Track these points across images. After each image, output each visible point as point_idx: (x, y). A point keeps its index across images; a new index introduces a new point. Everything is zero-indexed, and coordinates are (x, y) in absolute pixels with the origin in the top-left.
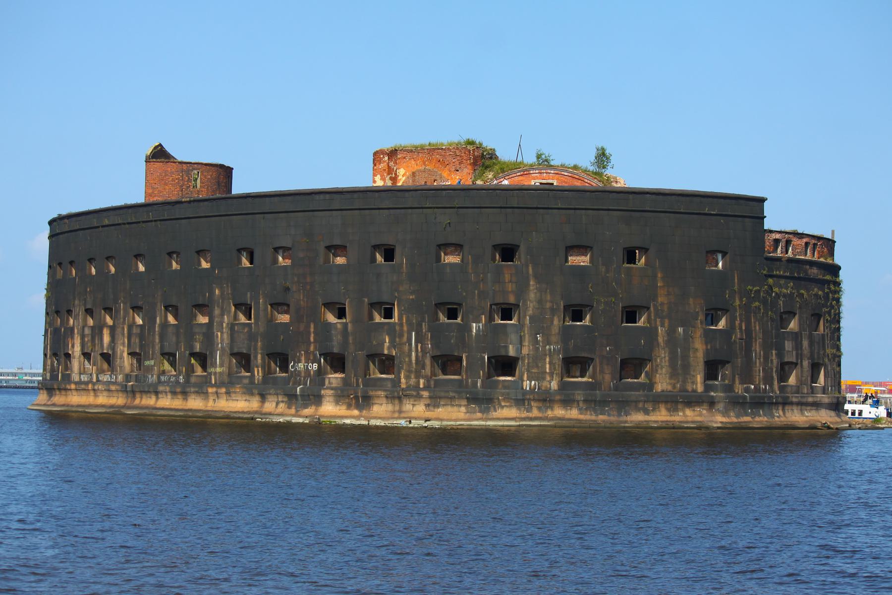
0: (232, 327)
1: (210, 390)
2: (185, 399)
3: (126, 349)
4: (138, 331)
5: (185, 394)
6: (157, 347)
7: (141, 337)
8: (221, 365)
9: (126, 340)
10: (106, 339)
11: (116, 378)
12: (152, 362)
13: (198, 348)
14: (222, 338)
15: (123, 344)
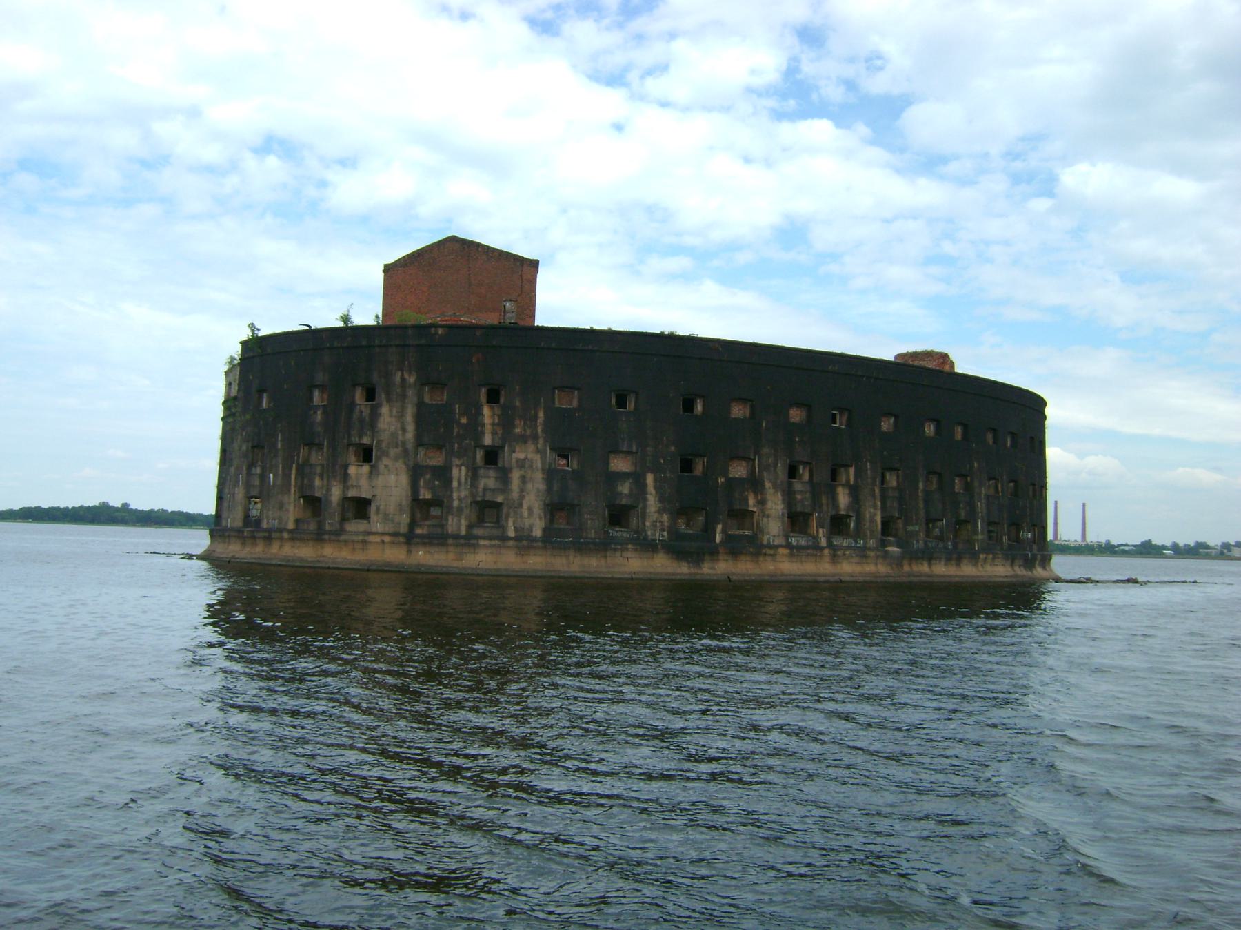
0: (988, 497)
1: (982, 556)
2: (958, 565)
3: (879, 513)
4: (897, 494)
5: (959, 561)
6: (922, 513)
9: (879, 503)
10: (843, 498)
11: (865, 542)
12: (917, 528)
13: (963, 515)
14: (981, 506)
15: (875, 507)
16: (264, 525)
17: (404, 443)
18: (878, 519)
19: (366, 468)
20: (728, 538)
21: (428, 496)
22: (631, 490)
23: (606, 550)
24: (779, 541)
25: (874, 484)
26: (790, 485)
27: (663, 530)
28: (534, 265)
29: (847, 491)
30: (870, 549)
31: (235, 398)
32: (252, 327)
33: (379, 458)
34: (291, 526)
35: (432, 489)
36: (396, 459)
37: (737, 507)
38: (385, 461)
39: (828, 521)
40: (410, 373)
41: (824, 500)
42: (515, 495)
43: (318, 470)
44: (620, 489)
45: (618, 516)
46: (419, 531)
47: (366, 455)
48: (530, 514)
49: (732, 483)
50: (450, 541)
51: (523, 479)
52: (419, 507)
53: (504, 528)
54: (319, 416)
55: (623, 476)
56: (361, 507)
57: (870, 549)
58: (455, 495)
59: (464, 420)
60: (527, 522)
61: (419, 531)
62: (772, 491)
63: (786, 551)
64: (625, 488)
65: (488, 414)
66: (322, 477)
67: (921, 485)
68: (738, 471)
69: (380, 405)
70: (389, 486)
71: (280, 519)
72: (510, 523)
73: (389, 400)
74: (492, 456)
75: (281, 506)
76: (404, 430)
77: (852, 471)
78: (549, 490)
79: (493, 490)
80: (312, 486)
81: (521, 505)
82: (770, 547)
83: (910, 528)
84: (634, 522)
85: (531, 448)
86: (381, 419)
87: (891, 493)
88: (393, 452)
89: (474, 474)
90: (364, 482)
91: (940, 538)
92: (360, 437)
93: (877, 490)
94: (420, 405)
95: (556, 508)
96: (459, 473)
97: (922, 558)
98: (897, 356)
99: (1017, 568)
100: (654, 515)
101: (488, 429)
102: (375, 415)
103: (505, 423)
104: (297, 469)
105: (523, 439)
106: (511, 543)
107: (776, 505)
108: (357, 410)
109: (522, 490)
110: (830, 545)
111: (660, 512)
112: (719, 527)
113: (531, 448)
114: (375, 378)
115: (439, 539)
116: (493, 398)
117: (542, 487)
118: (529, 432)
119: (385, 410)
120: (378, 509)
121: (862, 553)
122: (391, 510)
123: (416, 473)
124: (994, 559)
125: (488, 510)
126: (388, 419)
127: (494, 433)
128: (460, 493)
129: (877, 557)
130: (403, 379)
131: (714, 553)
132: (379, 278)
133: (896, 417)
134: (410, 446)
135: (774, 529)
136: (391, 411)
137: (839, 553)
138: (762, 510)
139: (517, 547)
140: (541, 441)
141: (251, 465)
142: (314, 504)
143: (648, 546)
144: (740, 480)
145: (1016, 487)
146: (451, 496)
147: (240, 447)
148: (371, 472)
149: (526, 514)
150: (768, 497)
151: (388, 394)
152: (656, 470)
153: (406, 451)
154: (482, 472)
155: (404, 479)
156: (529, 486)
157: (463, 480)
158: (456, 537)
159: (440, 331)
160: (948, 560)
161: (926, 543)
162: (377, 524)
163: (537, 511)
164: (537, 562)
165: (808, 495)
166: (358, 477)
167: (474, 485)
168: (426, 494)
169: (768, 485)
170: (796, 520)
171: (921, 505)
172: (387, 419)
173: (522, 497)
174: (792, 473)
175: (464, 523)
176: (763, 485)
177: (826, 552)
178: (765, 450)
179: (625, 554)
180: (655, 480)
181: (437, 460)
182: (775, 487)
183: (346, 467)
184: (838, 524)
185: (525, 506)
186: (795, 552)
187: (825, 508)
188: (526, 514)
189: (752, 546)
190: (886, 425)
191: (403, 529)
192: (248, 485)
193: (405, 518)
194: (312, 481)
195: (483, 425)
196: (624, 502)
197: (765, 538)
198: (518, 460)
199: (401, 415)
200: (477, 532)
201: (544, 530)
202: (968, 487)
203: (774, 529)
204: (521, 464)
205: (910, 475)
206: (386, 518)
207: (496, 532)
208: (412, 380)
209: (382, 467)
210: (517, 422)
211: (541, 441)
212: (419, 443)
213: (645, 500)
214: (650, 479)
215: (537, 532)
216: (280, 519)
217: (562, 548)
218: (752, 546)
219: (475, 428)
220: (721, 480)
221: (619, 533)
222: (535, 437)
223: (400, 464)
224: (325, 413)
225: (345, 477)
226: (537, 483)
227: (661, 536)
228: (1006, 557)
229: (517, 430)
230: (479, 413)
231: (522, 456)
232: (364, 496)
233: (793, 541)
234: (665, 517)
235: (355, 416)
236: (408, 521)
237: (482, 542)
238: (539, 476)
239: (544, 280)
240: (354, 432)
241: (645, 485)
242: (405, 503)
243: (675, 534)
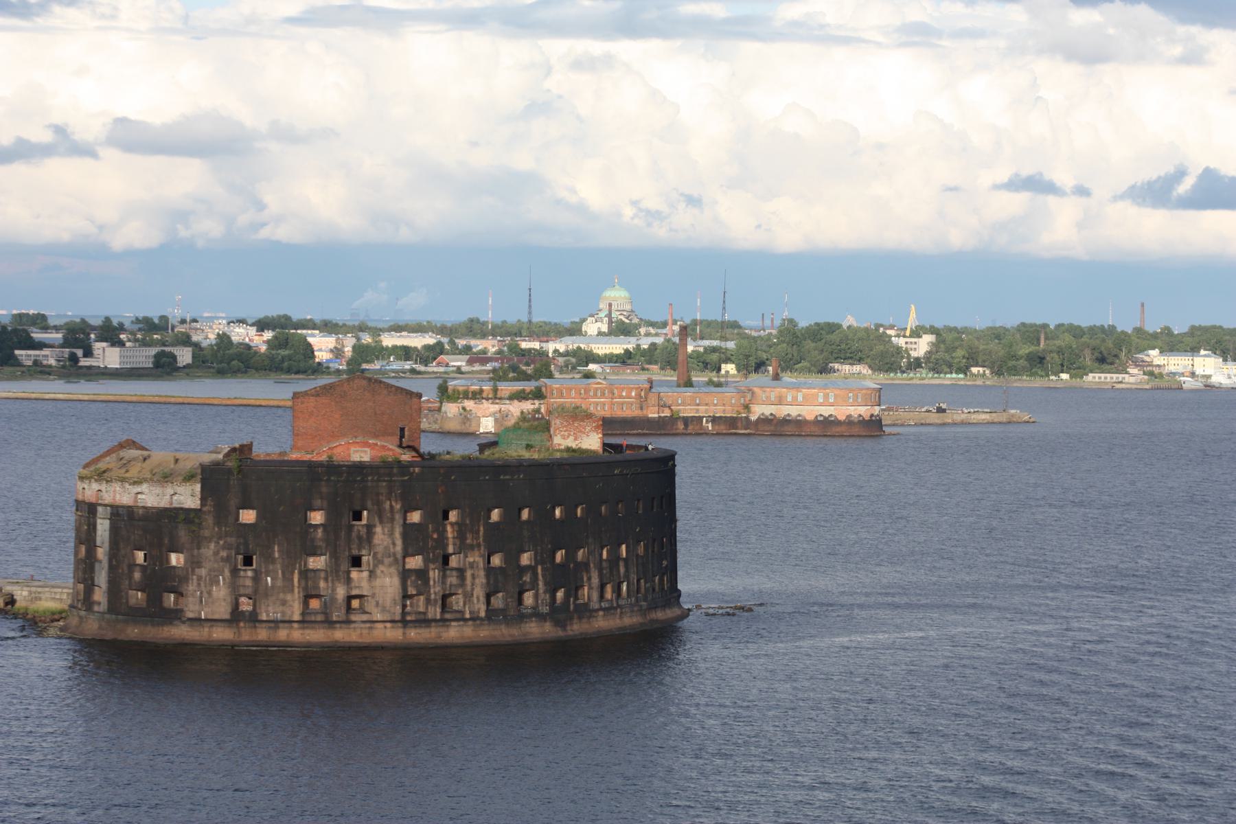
17: (394, 554)
24: (597, 606)
34: (297, 617)
35: (416, 587)
36: (390, 565)
42: (469, 588)
43: (323, 575)
51: (473, 577)
59: (435, 536)
60: (477, 607)
66: (326, 579)
69: (375, 526)
70: (388, 585)
71: (283, 613)
73: (381, 522)
75: (284, 603)
76: (394, 544)
77: (624, 546)
78: (488, 583)
85: (477, 553)
88: (387, 561)
89: (444, 577)
90: (365, 584)
92: (359, 550)
96: (434, 574)
101: (451, 541)
104: (300, 573)
105: (472, 547)
111: (545, 592)
113: (477, 553)
117: (484, 581)
119: (378, 529)
122: (388, 603)
123: (405, 574)
126: (381, 537)
127: (454, 544)
130: (391, 506)
134: (399, 556)
147: (216, 553)
152: (542, 563)
153: (396, 560)
155: (396, 581)
156: (477, 581)
158: (435, 621)
164: (485, 633)
166: (360, 580)
167: (444, 583)
173: (473, 589)
175: (439, 610)
178: (590, 540)
183: (349, 572)
191: (398, 617)
199: (391, 534)
200: (448, 616)
204: (472, 565)
206: (384, 610)
208: (398, 506)
209: (378, 572)
214: (540, 568)
215: (483, 614)
218: (585, 611)
222: (479, 545)
223: (393, 570)
225: (349, 580)
229: (468, 541)
230: (445, 531)
231: (471, 560)
235: (354, 534)
237: (453, 624)
238: (482, 573)
240: (354, 546)
242: (398, 598)
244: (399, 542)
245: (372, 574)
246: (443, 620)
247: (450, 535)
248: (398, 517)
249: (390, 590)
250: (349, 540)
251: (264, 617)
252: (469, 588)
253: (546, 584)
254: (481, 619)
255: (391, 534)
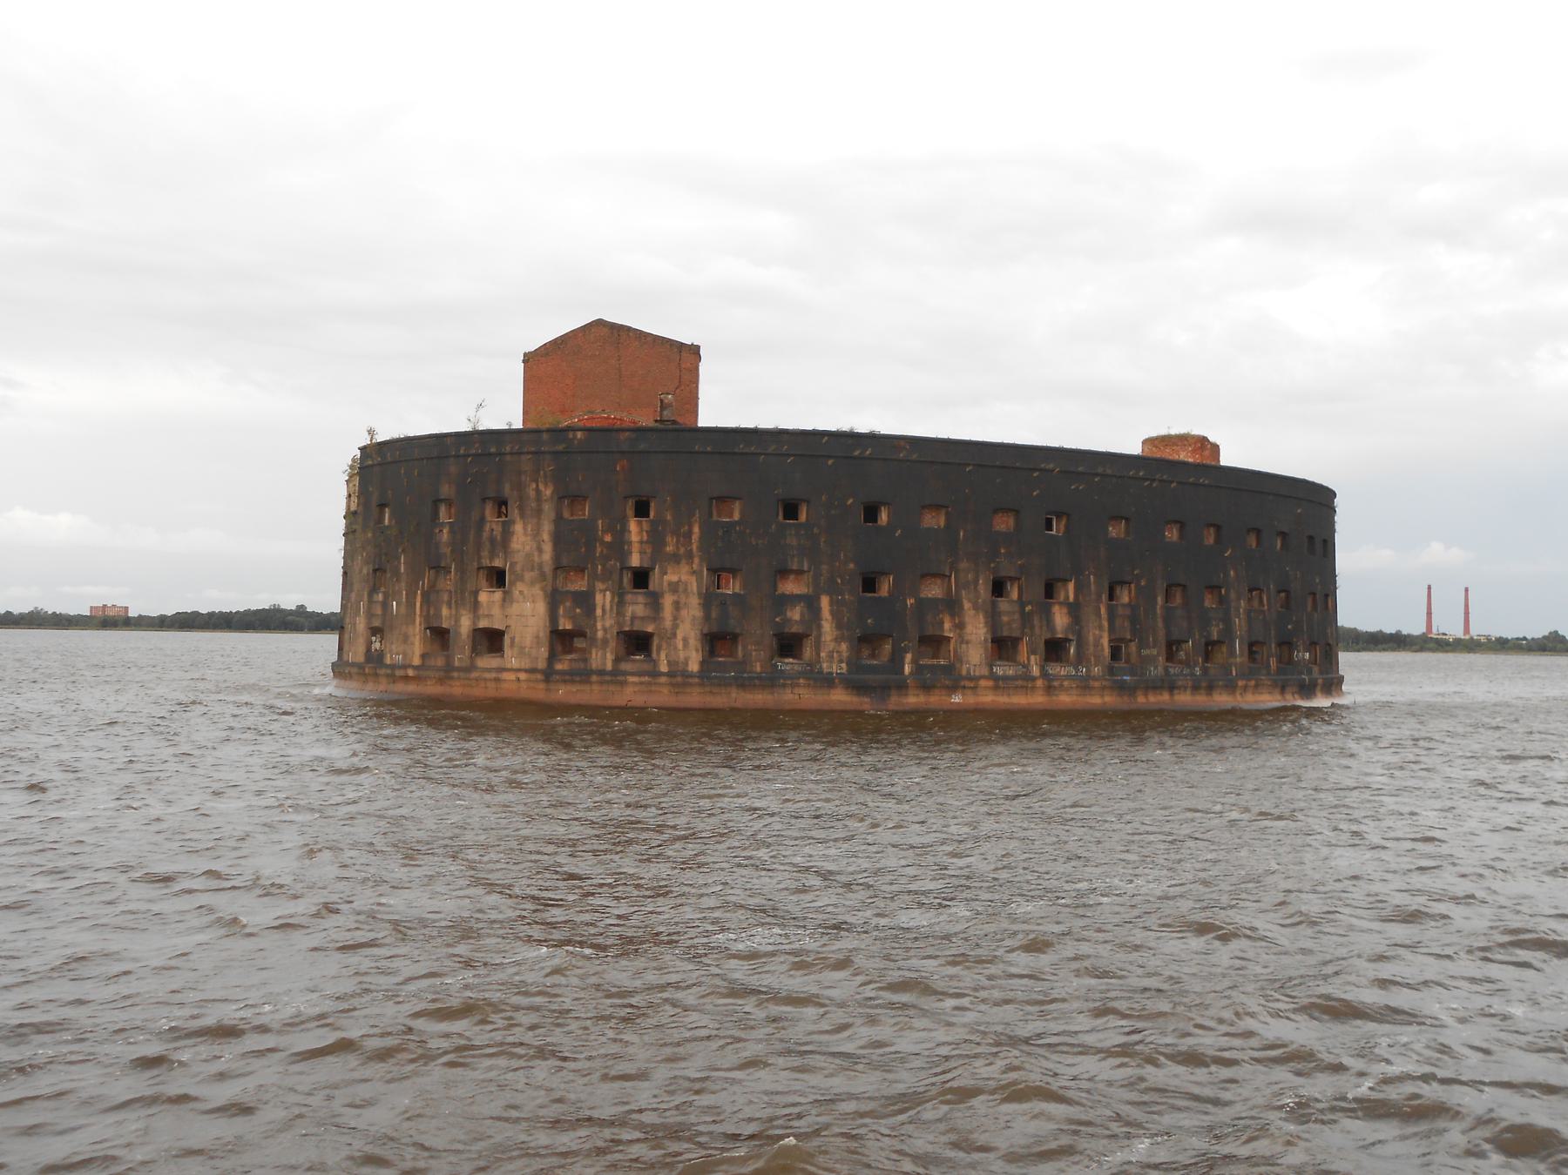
0: (1248, 612)
1: (1240, 683)
4: (1128, 612)
5: (1210, 689)
6: (1161, 634)
7: (1134, 620)
8: (1241, 655)
9: (1106, 624)
10: (1060, 619)
12: (1155, 652)
14: (1239, 623)
15: (1100, 627)
16: (388, 661)
17: (540, 566)
18: (1105, 642)
19: (498, 595)
20: (918, 669)
21: (569, 627)
22: (802, 614)
23: (773, 686)
25: (1099, 599)
26: (994, 604)
27: (841, 661)
28: (695, 351)
29: (1065, 610)
30: (1095, 679)
31: (355, 513)
32: (371, 432)
33: (512, 583)
34: (417, 661)
35: (573, 618)
36: (532, 583)
37: (930, 631)
38: (520, 586)
39: (1042, 646)
40: (546, 485)
41: (1036, 622)
42: (668, 623)
43: (446, 597)
44: (789, 614)
45: (788, 645)
46: (559, 667)
47: (498, 578)
48: (684, 645)
49: (921, 603)
50: (594, 678)
51: (677, 606)
52: (561, 640)
53: (655, 663)
54: (445, 535)
55: (793, 599)
56: (492, 640)
57: (1095, 679)
58: (599, 626)
59: (608, 538)
61: (559, 667)
62: (972, 612)
63: (991, 683)
64: (795, 614)
65: (635, 530)
67: (1160, 600)
68: (933, 590)
69: (513, 522)
70: (525, 615)
72: (663, 656)
73: (522, 516)
74: (641, 578)
75: (406, 639)
76: (540, 550)
77: (1071, 586)
78: (707, 617)
79: (642, 618)
80: (438, 616)
81: (675, 635)
82: (971, 679)
83: (1145, 652)
84: (808, 652)
86: (515, 539)
87: (1120, 611)
88: (528, 576)
89: (621, 603)
90: (496, 611)
91: (1187, 663)
93: (1103, 610)
94: (559, 519)
95: (717, 640)
96: (604, 600)
97: (1162, 688)
98: (1149, 442)
99: (1289, 697)
100: (830, 646)
101: (635, 548)
102: (507, 533)
103: (655, 539)
105: (676, 559)
106: (663, 679)
107: (977, 629)
108: (487, 528)
109: (675, 618)
110: (1044, 675)
111: (837, 640)
112: (909, 657)
113: (685, 568)
114: (507, 490)
115: (582, 675)
116: (642, 510)
118: (682, 550)
119: (518, 527)
120: (513, 640)
121: (1084, 685)
122: (528, 641)
123: (554, 600)
124: (1256, 686)
125: (638, 643)
126: (522, 539)
128: (605, 623)
129: (1103, 688)
131: (902, 687)
132: (520, 368)
133: (1127, 520)
134: (548, 569)
135: (974, 654)
136: (525, 529)
137: (1056, 684)
138: (960, 636)
139: (672, 685)
140: (696, 560)
141: (373, 590)
142: (440, 636)
143: (828, 682)
144: (935, 601)
145: (1287, 597)
146: (595, 625)
148: (504, 600)
149: (680, 645)
150: (967, 619)
151: (521, 509)
152: (832, 590)
154: (629, 597)
155: (541, 607)
156: (684, 613)
157: (608, 607)
158: (601, 672)
159: (579, 434)
160: (1196, 688)
161: (1166, 669)
162: (511, 659)
163: (694, 642)
165: (1016, 616)
167: (620, 613)
168: (565, 624)
169: (967, 605)
170: (1002, 646)
171: (1160, 624)
172: (521, 539)
173: (675, 626)
174: (998, 588)
175: (610, 657)
176: (961, 607)
177: (1039, 683)
178: (964, 565)
179: (796, 691)
180: (831, 603)
181: (580, 585)
182: (976, 607)
183: (476, 593)
184: (1054, 650)
185: (680, 636)
186: (1000, 684)
187: (1037, 630)
188: (680, 645)
189: (953, 678)
190: (1115, 531)
191: (542, 665)
192: (370, 615)
193: (544, 652)
194: (438, 611)
195: (630, 543)
196: (794, 629)
197: (965, 667)
198: (670, 584)
199: (537, 533)
200: (625, 666)
201: (702, 663)
202: (1222, 601)
203: (974, 654)
204: (674, 588)
205: (1175, 582)
206: (522, 653)
207: (646, 667)
208: (548, 492)
209: (516, 593)
210: (669, 539)
211: (696, 560)
212: (558, 568)
213: (819, 627)
214: (825, 602)
215: (694, 667)
216: (405, 655)
217: (724, 683)
219: (620, 548)
220: (910, 601)
221: (788, 664)
223: (537, 591)
224: (452, 532)
225: (476, 605)
226: (693, 609)
227: (838, 668)
228: (1274, 685)
229: (669, 549)
230: (625, 529)
231: (675, 578)
232: (496, 626)
233: (999, 671)
234: (844, 646)
235: (485, 535)
236: (546, 655)
237: (631, 679)
238: (694, 601)
239: (707, 371)
240: (485, 553)
241: (819, 609)
242: (544, 634)
243: (854, 665)
244: (548, 548)
245: (507, 599)
246: (615, 672)
247: (634, 538)
248: (547, 508)
249: (532, 621)
250: (479, 546)
251: (457, 664)
252: (668, 623)
253: (839, 625)
254: (686, 675)
255: (537, 533)
